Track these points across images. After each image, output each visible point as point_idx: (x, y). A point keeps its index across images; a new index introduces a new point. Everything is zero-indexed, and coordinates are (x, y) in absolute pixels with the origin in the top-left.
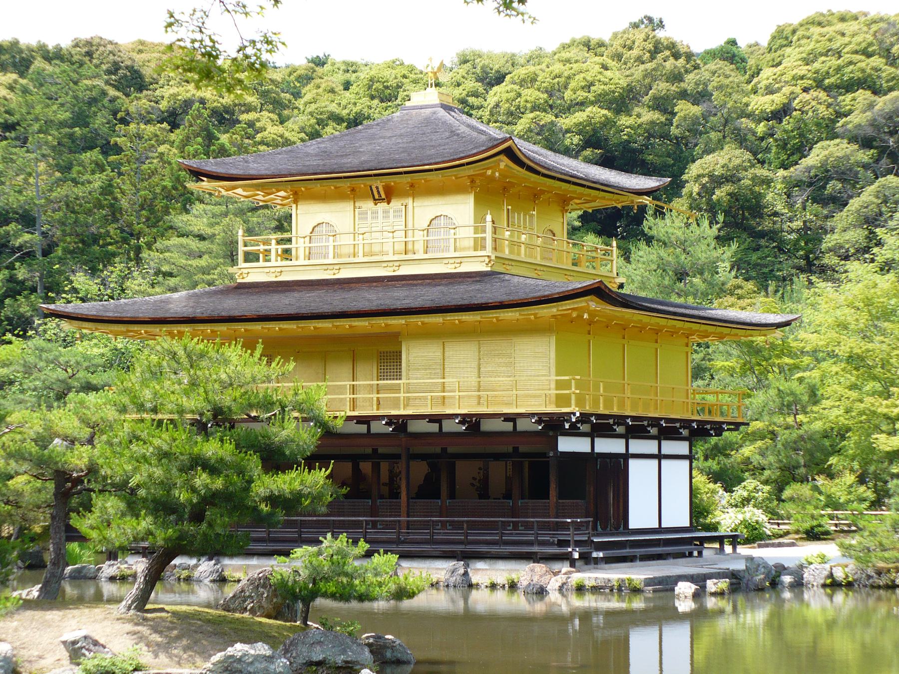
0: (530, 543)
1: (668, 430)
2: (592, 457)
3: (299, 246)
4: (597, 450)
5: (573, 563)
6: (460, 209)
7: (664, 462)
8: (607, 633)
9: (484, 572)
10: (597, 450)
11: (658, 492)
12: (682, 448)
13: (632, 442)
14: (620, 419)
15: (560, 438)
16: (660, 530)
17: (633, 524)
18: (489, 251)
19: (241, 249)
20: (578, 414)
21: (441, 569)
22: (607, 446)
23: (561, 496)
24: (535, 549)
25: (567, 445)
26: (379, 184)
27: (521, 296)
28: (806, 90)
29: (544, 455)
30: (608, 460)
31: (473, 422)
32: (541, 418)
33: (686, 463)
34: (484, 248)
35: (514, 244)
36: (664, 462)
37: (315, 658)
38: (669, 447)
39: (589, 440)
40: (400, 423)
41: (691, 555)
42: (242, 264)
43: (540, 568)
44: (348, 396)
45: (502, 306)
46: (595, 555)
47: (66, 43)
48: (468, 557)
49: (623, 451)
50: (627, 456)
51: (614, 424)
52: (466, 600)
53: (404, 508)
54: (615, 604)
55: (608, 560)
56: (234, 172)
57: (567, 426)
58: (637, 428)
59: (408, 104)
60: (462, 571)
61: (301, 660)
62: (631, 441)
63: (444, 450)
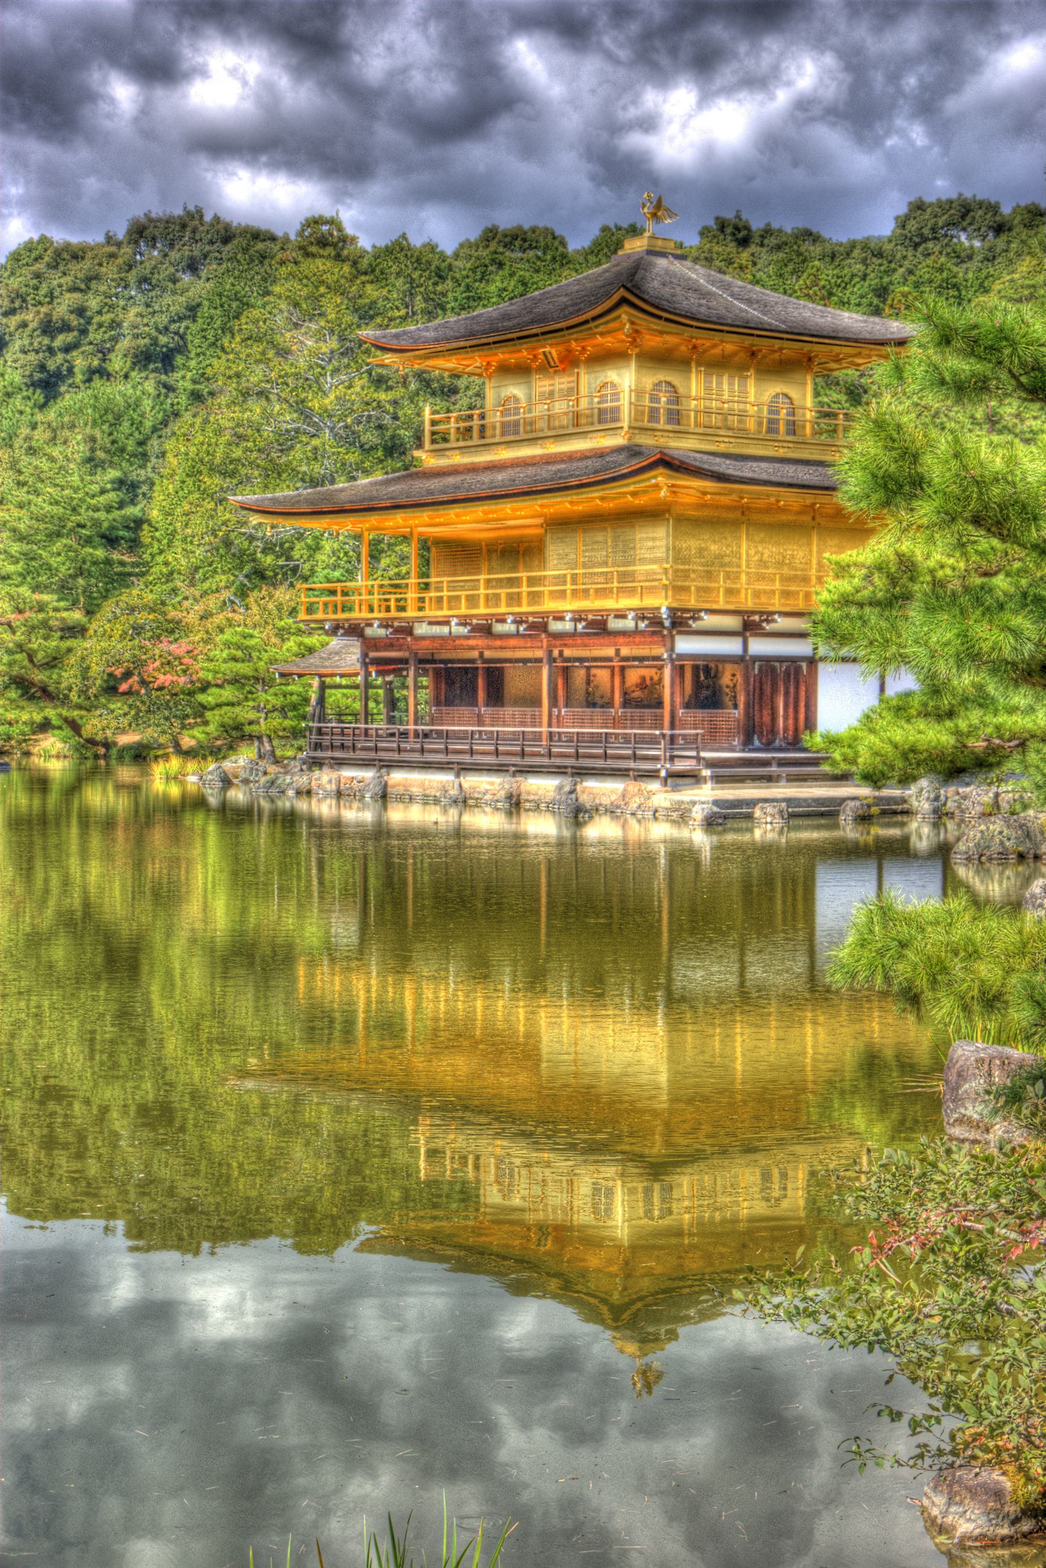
5: (665, 783)
14: (768, 616)
20: (663, 610)
22: (759, 647)
24: (632, 765)
25: (685, 645)
30: (777, 664)
43: (632, 786)
48: (582, 773)
50: (812, 661)
51: (762, 621)
55: (718, 779)
57: (667, 623)
59: (620, 253)
60: (567, 789)
63: (618, 651)
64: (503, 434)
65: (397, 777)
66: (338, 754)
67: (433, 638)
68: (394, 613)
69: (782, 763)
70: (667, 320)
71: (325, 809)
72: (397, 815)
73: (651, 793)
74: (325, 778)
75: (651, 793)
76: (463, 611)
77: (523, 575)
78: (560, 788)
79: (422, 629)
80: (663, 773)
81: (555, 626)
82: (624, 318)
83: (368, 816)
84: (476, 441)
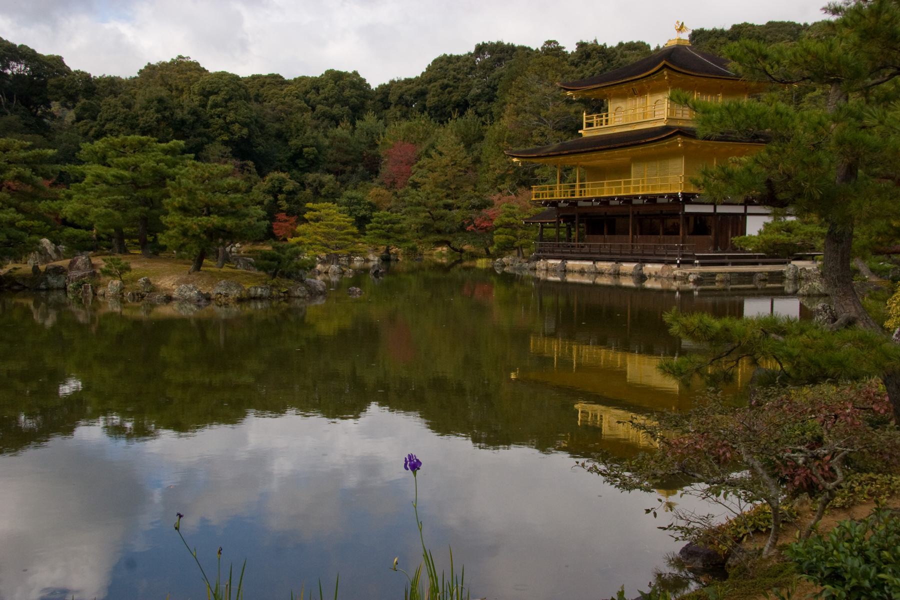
0: (664, 256)
2: (715, 215)
5: (679, 266)
9: (650, 268)
19: (585, 121)
22: (721, 209)
24: (666, 258)
25: (689, 209)
31: (652, 200)
32: (670, 196)
39: (712, 207)
40: (628, 200)
41: (785, 263)
43: (667, 267)
47: (727, 27)
50: (744, 215)
55: (702, 264)
65: (570, 263)
66: (548, 254)
67: (586, 207)
68: (569, 197)
69: (730, 257)
71: (541, 275)
72: (570, 279)
73: (674, 270)
74: (541, 264)
75: (674, 270)
76: (597, 196)
77: (622, 180)
78: (635, 267)
79: (580, 204)
82: (665, 73)
83: (558, 279)
84: (604, 126)
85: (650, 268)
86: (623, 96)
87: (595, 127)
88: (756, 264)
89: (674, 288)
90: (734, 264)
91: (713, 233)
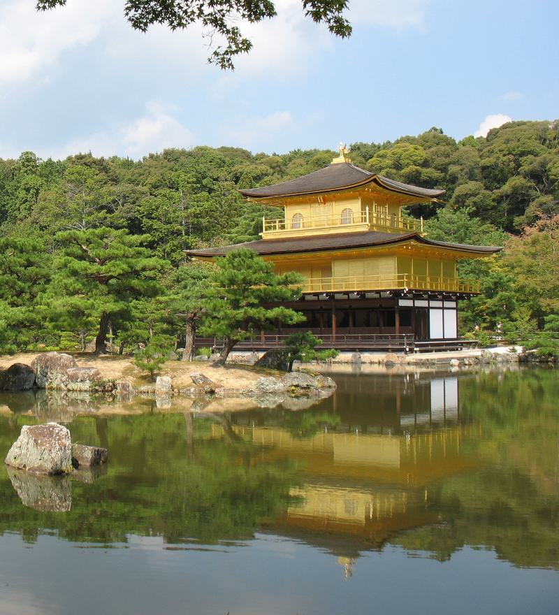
0: (388, 345)
1: (446, 298)
2: (414, 308)
3: (288, 222)
4: (416, 305)
5: (406, 353)
6: (355, 206)
7: (445, 311)
8: (421, 382)
10: (416, 305)
11: (443, 323)
12: (453, 304)
13: (431, 302)
14: (426, 292)
15: (400, 301)
16: (444, 339)
17: (432, 337)
18: (368, 222)
21: (348, 356)
22: (419, 303)
23: (401, 325)
24: (390, 347)
25: (402, 303)
26: (320, 198)
27: (381, 240)
28: (504, 155)
29: (394, 308)
31: (362, 294)
33: (455, 311)
34: (365, 221)
35: (378, 219)
36: (445, 311)
37: (294, 384)
38: (447, 304)
40: (331, 295)
41: (457, 350)
42: (264, 231)
44: (309, 284)
45: (374, 245)
46: (415, 349)
48: (362, 350)
49: (427, 306)
50: (429, 308)
52: (360, 368)
53: (334, 331)
54: (424, 370)
55: (421, 352)
56: (260, 194)
58: (433, 296)
60: (358, 357)
61: (288, 384)
62: (431, 302)
63: (350, 306)
64: (304, 227)
69: (432, 345)
70: (384, 187)
78: (354, 356)
80: (407, 349)
81: (337, 297)
85: (366, 356)
86: (291, 204)
87: (278, 230)
88: (445, 350)
89: (403, 373)
90: (436, 351)
91: (413, 325)
